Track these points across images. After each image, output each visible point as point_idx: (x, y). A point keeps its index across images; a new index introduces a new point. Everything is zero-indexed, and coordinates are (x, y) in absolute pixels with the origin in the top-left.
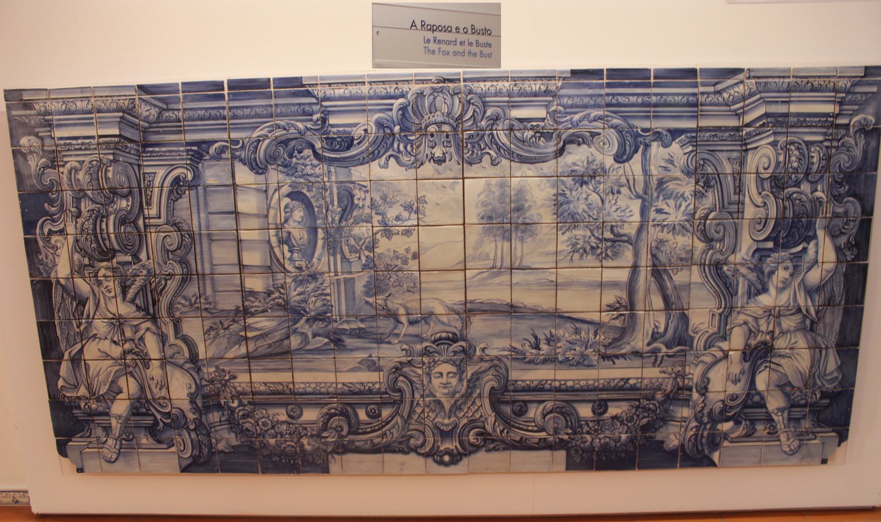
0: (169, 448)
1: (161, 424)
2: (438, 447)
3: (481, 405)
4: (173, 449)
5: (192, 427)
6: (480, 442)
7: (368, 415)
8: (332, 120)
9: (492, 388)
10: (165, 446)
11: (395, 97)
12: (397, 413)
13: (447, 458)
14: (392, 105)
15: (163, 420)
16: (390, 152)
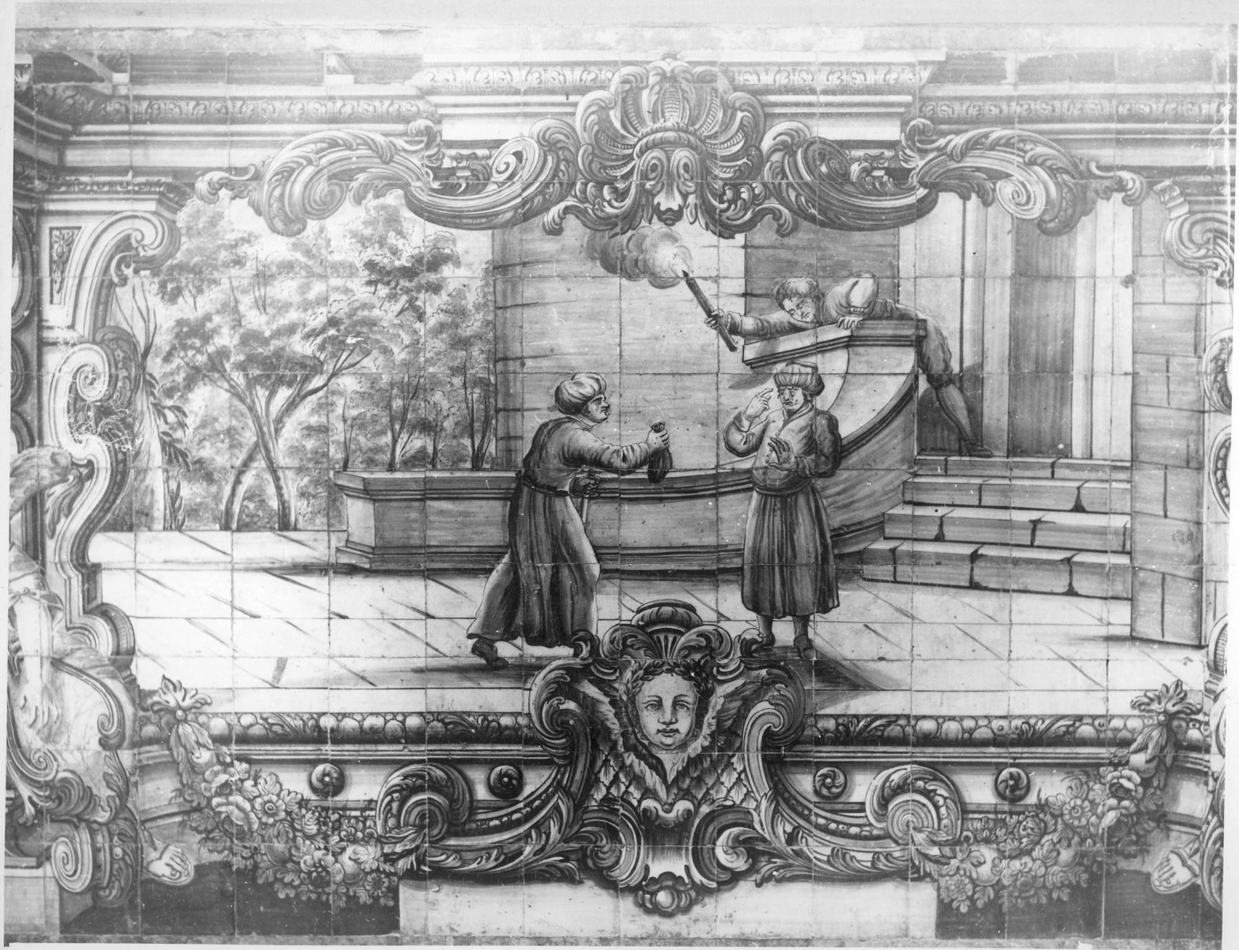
0: (38, 866)
1: (29, 809)
2: (647, 869)
3: (744, 770)
4: (48, 869)
5: (103, 816)
6: (740, 864)
7: (491, 789)
8: (450, 131)
9: (768, 734)
10: (32, 861)
11: (582, 90)
12: (557, 786)
13: (663, 898)
14: (575, 105)
15: (35, 799)
16: (570, 201)
